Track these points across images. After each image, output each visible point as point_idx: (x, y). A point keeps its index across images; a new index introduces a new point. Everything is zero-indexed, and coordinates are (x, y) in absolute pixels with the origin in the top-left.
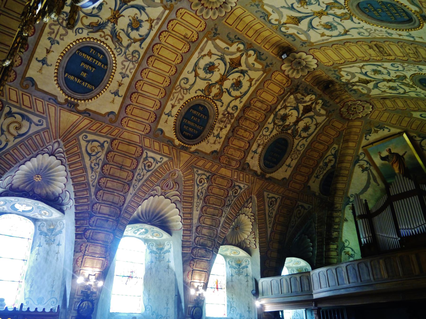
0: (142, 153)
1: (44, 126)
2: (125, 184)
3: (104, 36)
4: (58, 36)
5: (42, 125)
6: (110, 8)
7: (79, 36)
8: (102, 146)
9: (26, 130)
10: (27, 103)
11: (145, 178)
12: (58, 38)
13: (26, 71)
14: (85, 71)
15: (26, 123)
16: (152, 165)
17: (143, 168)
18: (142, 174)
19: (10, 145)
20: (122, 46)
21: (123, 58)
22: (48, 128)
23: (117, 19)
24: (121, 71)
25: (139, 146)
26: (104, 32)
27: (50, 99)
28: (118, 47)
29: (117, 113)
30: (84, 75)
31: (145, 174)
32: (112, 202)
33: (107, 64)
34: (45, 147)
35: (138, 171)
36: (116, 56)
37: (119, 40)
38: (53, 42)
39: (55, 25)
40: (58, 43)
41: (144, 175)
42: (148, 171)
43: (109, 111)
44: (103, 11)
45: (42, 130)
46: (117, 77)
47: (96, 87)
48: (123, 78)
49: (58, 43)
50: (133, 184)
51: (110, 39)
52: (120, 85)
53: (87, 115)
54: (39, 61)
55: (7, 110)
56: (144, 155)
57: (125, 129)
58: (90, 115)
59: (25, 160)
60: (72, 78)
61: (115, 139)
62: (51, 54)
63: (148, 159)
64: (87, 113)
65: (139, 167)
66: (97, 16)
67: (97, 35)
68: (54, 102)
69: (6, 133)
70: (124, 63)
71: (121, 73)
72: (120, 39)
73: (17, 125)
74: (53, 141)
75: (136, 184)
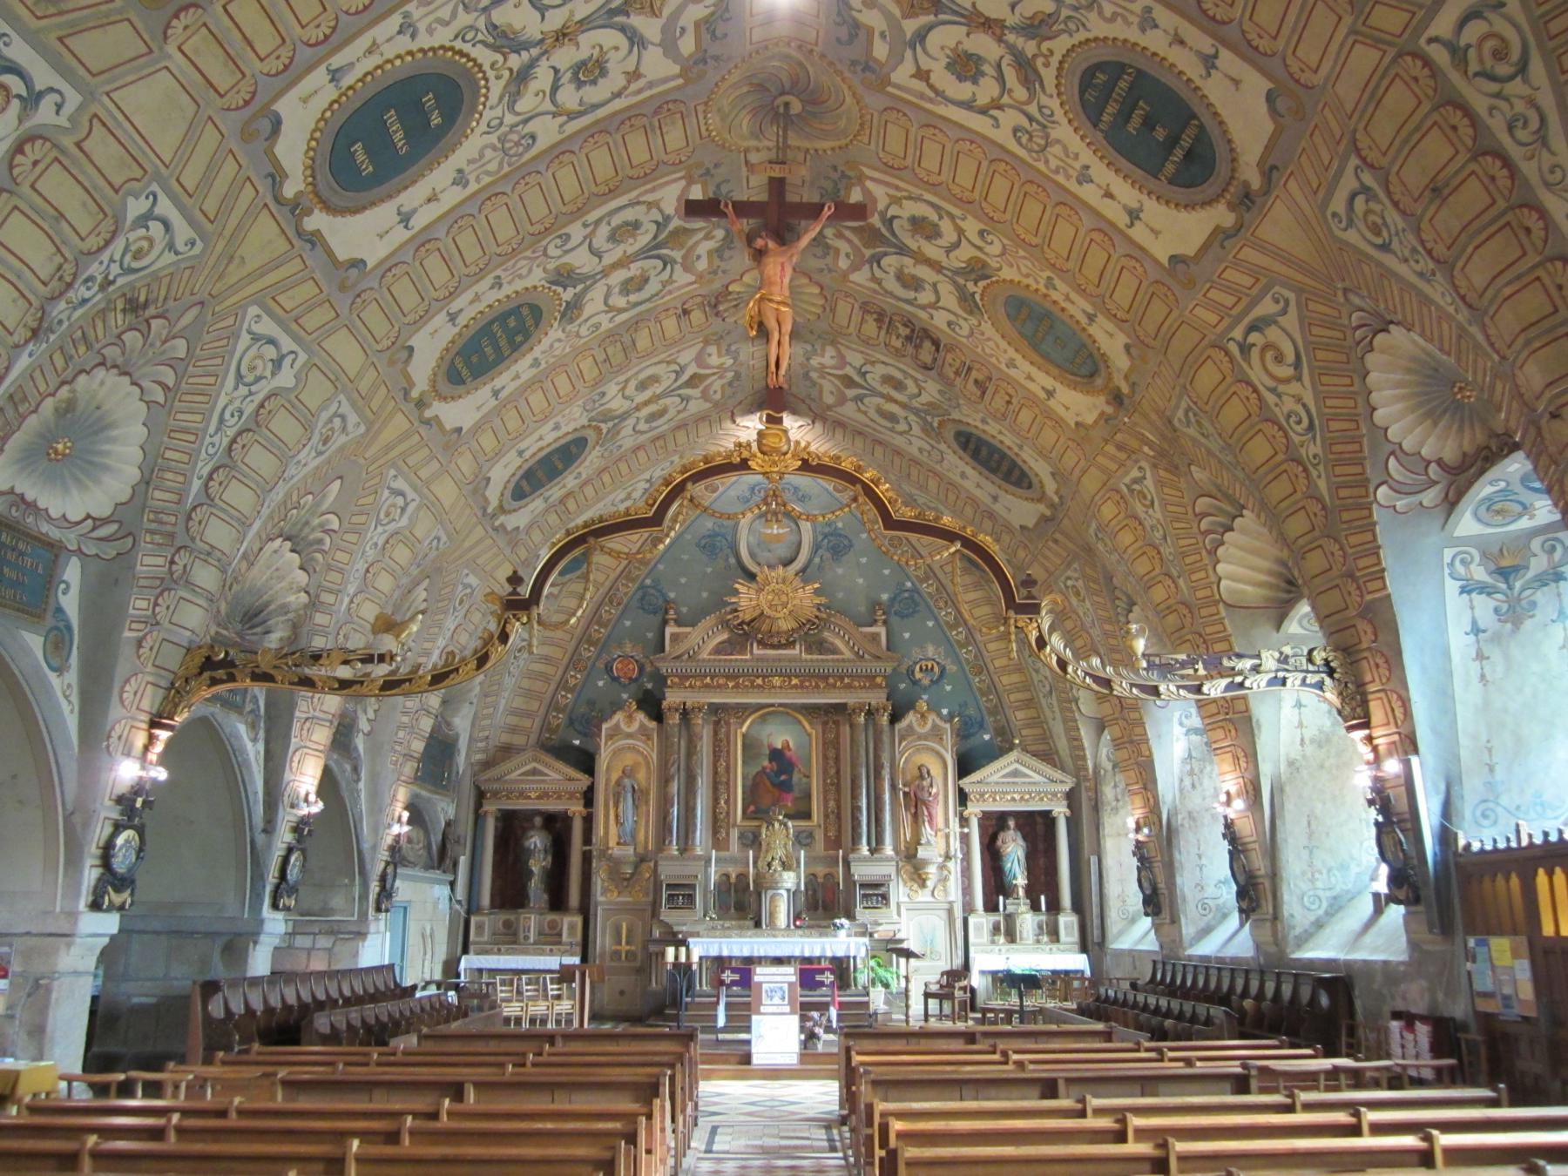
0: (1427, 62)
1: (1292, 296)
2: (1509, 217)
3: (1045, 56)
4: (1069, 161)
5: (1287, 302)
6: (968, 35)
7: (1059, 114)
8: (1365, 190)
9: (1290, 344)
10: (1229, 300)
11: (1547, 100)
12: (1077, 165)
13: (1156, 262)
14: (1149, 124)
15: (1273, 334)
16: (1503, 40)
17: (1494, 87)
18: (1520, 106)
19: (1309, 399)
20: (1057, 12)
21: (1093, 16)
22: (1299, 291)
23: (988, 19)
24: (1135, 27)
25: (1394, 61)
26: (1035, 56)
27: (1223, 247)
28: (1062, 26)
29: (1272, 86)
30: (1160, 134)
31: (1526, 91)
32: (1523, 330)
33: (1122, 67)
34: (1349, 333)
35: (1497, 124)
36: (1091, 36)
37: (1042, 21)
38: (1084, 178)
39: (1047, 162)
40: (1087, 167)
41: (1532, 103)
42: (1522, 68)
43: (1263, 108)
44: (982, 53)
45: (1298, 304)
46: (1155, 42)
47: (1194, 116)
48: (1156, 26)
49: (1087, 167)
50: (1534, 179)
51: (1045, 46)
52: (1182, 42)
53: (1275, 174)
54: (1132, 225)
55: (1234, 348)
56: (1440, 55)
57: (1327, 79)
58: (1274, 168)
59: (1360, 401)
60: (1170, 168)
61: (1354, 141)
62: (1114, 190)
63: (1463, 43)
64: (1269, 171)
65: (1480, 104)
66: (999, 66)
67: (1049, 75)
68: (1234, 240)
69: (1281, 388)
70: (1108, 14)
71: (1143, 30)
72: (1040, 17)
73: (1269, 355)
74: (1342, 300)
75: (1545, 168)
